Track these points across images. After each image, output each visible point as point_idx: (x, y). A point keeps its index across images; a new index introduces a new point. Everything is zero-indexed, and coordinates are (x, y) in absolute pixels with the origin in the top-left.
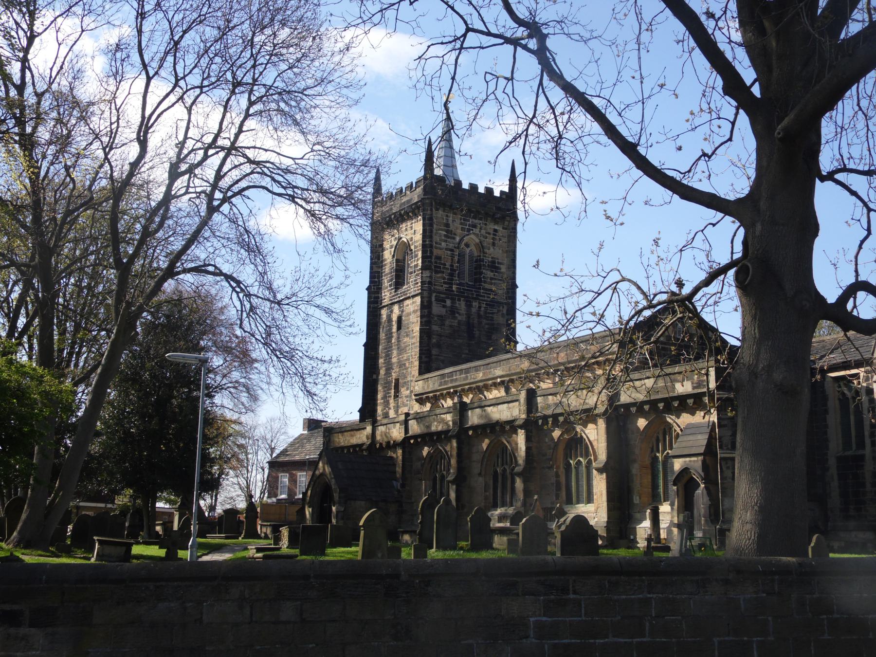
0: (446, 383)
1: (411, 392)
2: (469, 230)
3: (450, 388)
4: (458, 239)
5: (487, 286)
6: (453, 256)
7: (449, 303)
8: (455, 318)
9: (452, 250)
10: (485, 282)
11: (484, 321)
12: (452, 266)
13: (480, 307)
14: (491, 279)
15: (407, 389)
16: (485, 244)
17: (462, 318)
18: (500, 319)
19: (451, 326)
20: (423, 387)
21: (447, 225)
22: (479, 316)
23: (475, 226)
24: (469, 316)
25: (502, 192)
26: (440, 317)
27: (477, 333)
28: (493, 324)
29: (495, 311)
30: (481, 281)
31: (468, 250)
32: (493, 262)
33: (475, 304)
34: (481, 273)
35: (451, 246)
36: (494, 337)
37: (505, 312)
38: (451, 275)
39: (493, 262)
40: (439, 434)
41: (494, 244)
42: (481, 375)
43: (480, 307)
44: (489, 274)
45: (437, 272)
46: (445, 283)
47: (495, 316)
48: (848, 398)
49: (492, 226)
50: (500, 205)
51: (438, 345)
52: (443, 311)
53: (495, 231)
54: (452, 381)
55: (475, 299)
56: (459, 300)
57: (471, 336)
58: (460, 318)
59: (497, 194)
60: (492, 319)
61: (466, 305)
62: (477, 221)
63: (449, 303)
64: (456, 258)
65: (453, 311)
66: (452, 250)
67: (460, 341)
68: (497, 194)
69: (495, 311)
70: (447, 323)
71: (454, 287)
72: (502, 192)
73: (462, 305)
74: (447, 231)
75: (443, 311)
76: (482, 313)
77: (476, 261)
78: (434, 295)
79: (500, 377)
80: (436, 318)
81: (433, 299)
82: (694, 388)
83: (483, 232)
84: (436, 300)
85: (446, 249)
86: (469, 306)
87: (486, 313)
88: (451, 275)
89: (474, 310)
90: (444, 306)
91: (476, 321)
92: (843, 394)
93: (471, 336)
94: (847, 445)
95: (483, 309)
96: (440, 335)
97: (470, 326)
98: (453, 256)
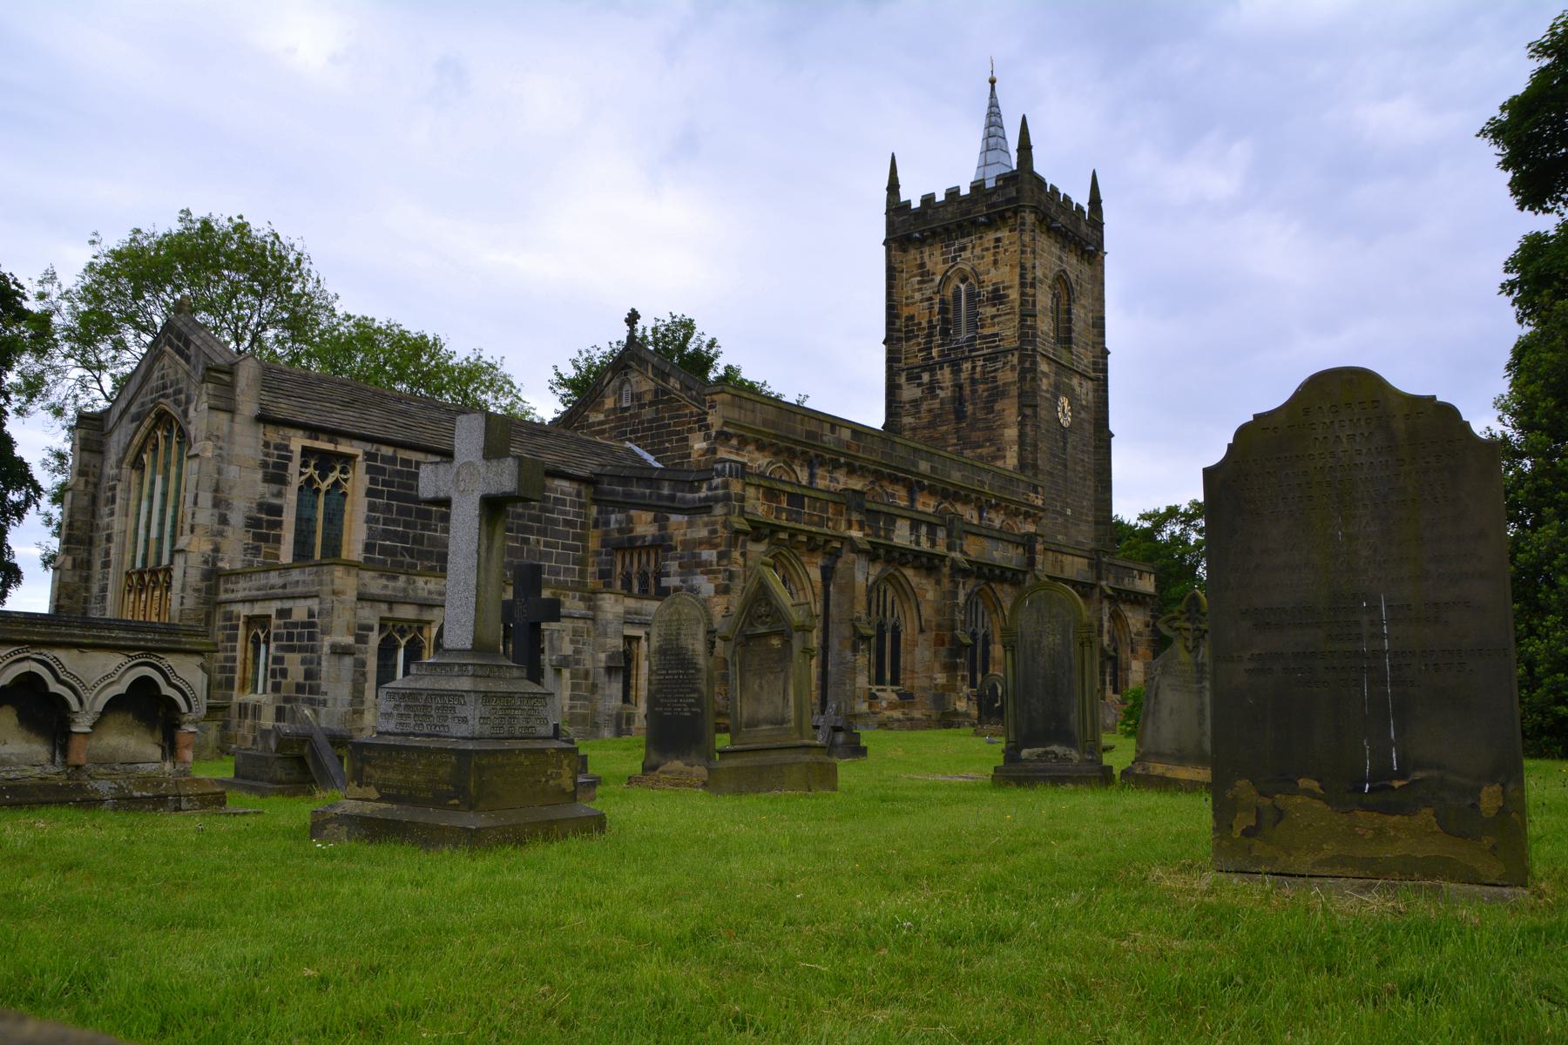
2: (954, 259)
4: (938, 278)
5: (987, 331)
6: (931, 308)
7: (926, 377)
8: (936, 396)
11: (981, 387)
12: (930, 321)
13: (974, 368)
14: (993, 317)
16: (981, 269)
21: (922, 265)
22: (973, 381)
23: (963, 249)
24: (959, 387)
26: (916, 403)
27: (969, 408)
29: (999, 365)
33: (967, 366)
35: (928, 293)
36: (997, 407)
39: (996, 290)
43: (974, 368)
44: (989, 311)
47: (999, 375)
49: (992, 236)
53: (998, 240)
55: (966, 359)
56: (941, 368)
60: (995, 379)
61: (953, 372)
62: (964, 241)
65: (932, 388)
66: (930, 299)
70: (925, 407)
71: (935, 352)
73: (945, 375)
74: (922, 275)
76: (977, 376)
83: (978, 251)
86: (956, 371)
87: (983, 373)
88: (930, 335)
90: (919, 385)
93: (960, 415)
96: (914, 429)
97: (958, 400)
98: (931, 308)
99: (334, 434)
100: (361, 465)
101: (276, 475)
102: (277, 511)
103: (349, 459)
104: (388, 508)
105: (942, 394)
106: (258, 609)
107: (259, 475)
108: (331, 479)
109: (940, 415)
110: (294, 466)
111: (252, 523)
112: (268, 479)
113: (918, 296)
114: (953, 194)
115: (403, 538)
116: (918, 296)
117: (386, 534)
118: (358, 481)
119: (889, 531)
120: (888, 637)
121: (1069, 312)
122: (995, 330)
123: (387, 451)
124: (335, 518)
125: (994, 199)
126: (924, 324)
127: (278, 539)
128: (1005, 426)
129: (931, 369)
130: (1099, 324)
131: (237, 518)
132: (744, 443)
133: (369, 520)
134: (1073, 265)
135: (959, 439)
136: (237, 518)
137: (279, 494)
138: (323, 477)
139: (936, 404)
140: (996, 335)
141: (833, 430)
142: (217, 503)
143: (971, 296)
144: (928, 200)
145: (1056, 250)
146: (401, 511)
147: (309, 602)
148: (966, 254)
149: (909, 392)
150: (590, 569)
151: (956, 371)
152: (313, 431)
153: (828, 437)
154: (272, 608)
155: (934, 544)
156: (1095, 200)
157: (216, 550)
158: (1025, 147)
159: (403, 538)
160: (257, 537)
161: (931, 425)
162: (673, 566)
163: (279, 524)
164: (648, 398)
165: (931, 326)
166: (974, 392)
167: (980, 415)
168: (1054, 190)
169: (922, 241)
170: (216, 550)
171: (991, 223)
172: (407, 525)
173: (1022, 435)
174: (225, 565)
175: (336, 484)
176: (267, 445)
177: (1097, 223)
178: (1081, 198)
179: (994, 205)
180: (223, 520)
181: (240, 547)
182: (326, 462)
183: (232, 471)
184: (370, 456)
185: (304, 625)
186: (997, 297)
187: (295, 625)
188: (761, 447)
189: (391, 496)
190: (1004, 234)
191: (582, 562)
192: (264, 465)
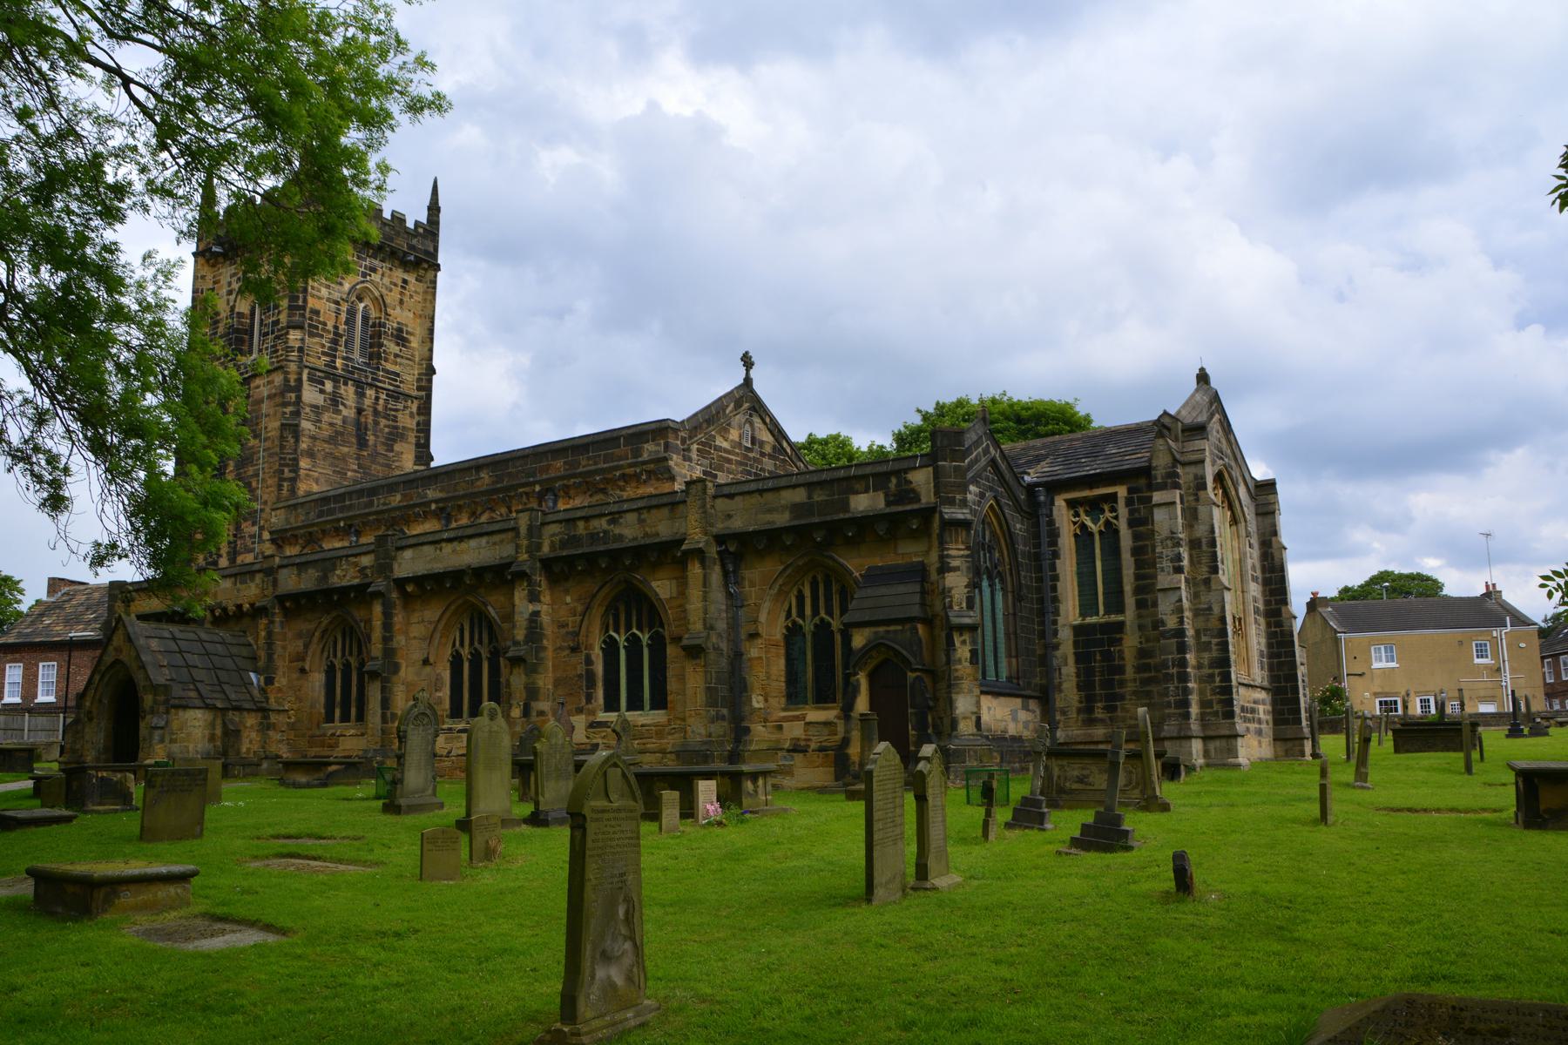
0: (331, 512)
1: (262, 528)
3: (338, 520)
5: (390, 367)
6: (338, 313)
7: (329, 386)
8: (338, 412)
9: (337, 303)
10: (386, 360)
11: (383, 422)
12: (336, 327)
13: (377, 398)
14: (396, 356)
15: (254, 524)
16: (388, 301)
17: (349, 413)
18: (407, 421)
19: (331, 424)
20: (287, 520)
22: (376, 412)
23: (374, 270)
24: (360, 411)
25: (417, 224)
27: (371, 439)
28: (396, 428)
29: (400, 406)
30: (379, 357)
31: (361, 306)
32: (400, 330)
33: (370, 393)
34: (381, 345)
35: (336, 296)
36: (397, 447)
37: (414, 409)
38: (335, 342)
40: (344, 591)
41: (401, 302)
42: (398, 497)
43: (377, 398)
45: (312, 335)
46: (324, 353)
47: (399, 415)
48: (1091, 534)
49: (399, 274)
50: (414, 242)
51: (310, 454)
52: (319, 400)
53: (405, 281)
54: (342, 509)
55: (371, 385)
56: (346, 384)
57: (362, 443)
58: (345, 412)
59: (410, 224)
60: (395, 419)
61: (357, 393)
62: (376, 262)
63: (329, 386)
64: (343, 316)
65: (335, 401)
66: (337, 303)
67: (346, 450)
68: (410, 224)
69: (400, 406)
70: (326, 417)
71: (339, 363)
72: (417, 224)
73: (348, 392)
76: (380, 408)
77: (374, 325)
78: (306, 371)
79: (436, 501)
80: (308, 410)
81: (305, 377)
82: (888, 504)
83: (386, 280)
84: (310, 379)
85: (328, 300)
86: (361, 395)
87: (386, 408)
88: (335, 342)
89: (368, 402)
90: (322, 391)
91: (370, 420)
92: (1083, 526)
93: (362, 443)
94: (1087, 606)
95: (381, 402)
96: (314, 438)
98: (338, 313)
105: (345, 412)
109: (342, 434)
120: (339, 675)
122: (397, 369)
125: (414, 242)
126: (330, 327)
129: (335, 379)
135: (360, 466)
139: (338, 420)
140: (398, 375)
143: (365, 318)
148: (376, 277)
151: (361, 395)
161: (332, 440)
166: (376, 423)
167: (381, 449)
179: (412, 247)
186: (400, 337)
190: (411, 278)
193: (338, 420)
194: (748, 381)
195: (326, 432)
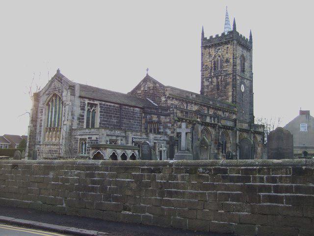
5: (225, 69)
6: (211, 63)
7: (210, 80)
21: (210, 53)
22: (222, 81)
24: (218, 82)
27: (220, 88)
36: (227, 87)
41: (227, 53)
49: (226, 46)
52: (208, 83)
53: (228, 47)
55: (220, 76)
58: (214, 84)
65: (212, 82)
70: (210, 87)
71: (212, 74)
73: (215, 80)
75: (208, 83)
86: (217, 79)
93: (218, 89)
97: (218, 85)
98: (211, 63)
99: (94, 100)
100: (99, 106)
101: (83, 109)
102: (83, 116)
103: (96, 105)
104: (104, 115)
106: (83, 137)
107: (80, 109)
108: (93, 108)
110: (86, 107)
111: (79, 119)
112: (82, 109)
113: (208, 60)
114: (217, 36)
115: (107, 121)
116: (208, 60)
117: (103, 121)
118: (98, 109)
119: (206, 119)
121: (244, 64)
122: (226, 69)
123: (103, 103)
124: (93, 117)
127: (83, 122)
128: (229, 92)
129: (211, 78)
130: (251, 67)
131: (76, 118)
132: (173, 98)
133: (100, 118)
134: (245, 53)
136: (76, 118)
137: (83, 113)
138: (91, 109)
139: (212, 86)
141: (192, 95)
142: (72, 115)
143: (221, 60)
144: (211, 37)
145: (241, 49)
146: (106, 116)
147: (96, 136)
149: (206, 83)
150: (143, 127)
152: (89, 99)
153: (191, 97)
154: (87, 137)
155: (215, 122)
156: (251, 37)
157: (72, 124)
158: (234, 25)
159: (107, 121)
160: (80, 122)
161: (211, 91)
162: (162, 127)
163: (83, 119)
164: (152, 88)
165: (212, 68)
168: (241, 35)
169: (209, 47)
170: (72, 124)
171: (226, 43)
172: (108, 118)
173: (233, 94)
174: (73, 128)
175: (94, 110)
176: (81, 102)
177: (251, 42)
178: (247, 37)
180: (73, 118)
181: (76, 124)
182: (91, 105)
183: (75, 108)
184: (100, 104)
185: (95, 140)
187: (93, 140)
188: (176, 100)
189: (105, 113)
190: (229, 46)
191: (141, 126)
192: (81, 106)
193: (212, 86)
194: (147, 75)
195: (210, 90)
